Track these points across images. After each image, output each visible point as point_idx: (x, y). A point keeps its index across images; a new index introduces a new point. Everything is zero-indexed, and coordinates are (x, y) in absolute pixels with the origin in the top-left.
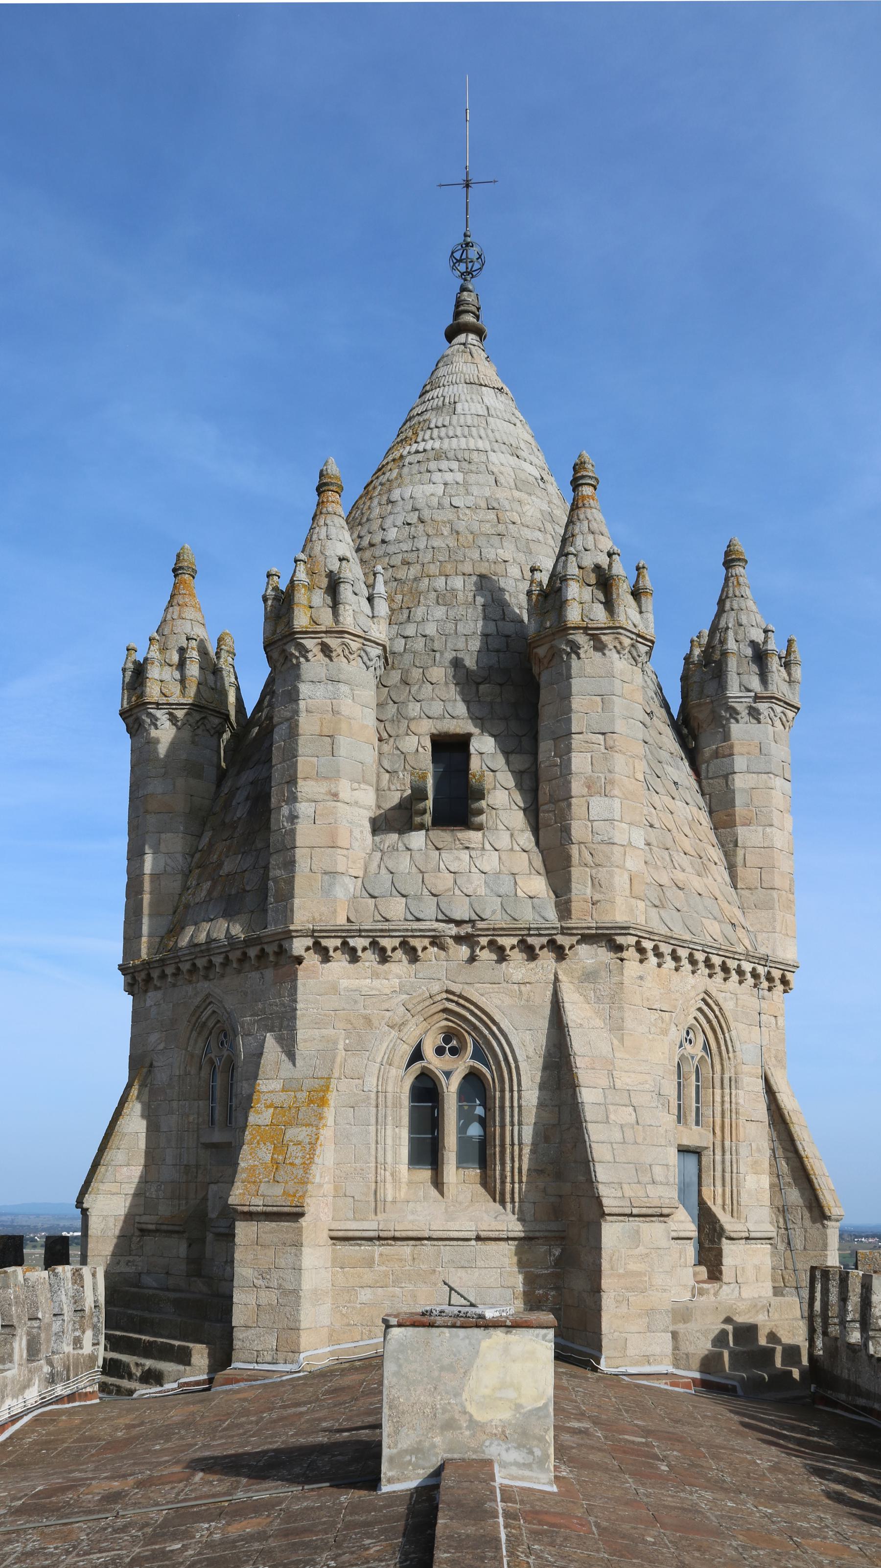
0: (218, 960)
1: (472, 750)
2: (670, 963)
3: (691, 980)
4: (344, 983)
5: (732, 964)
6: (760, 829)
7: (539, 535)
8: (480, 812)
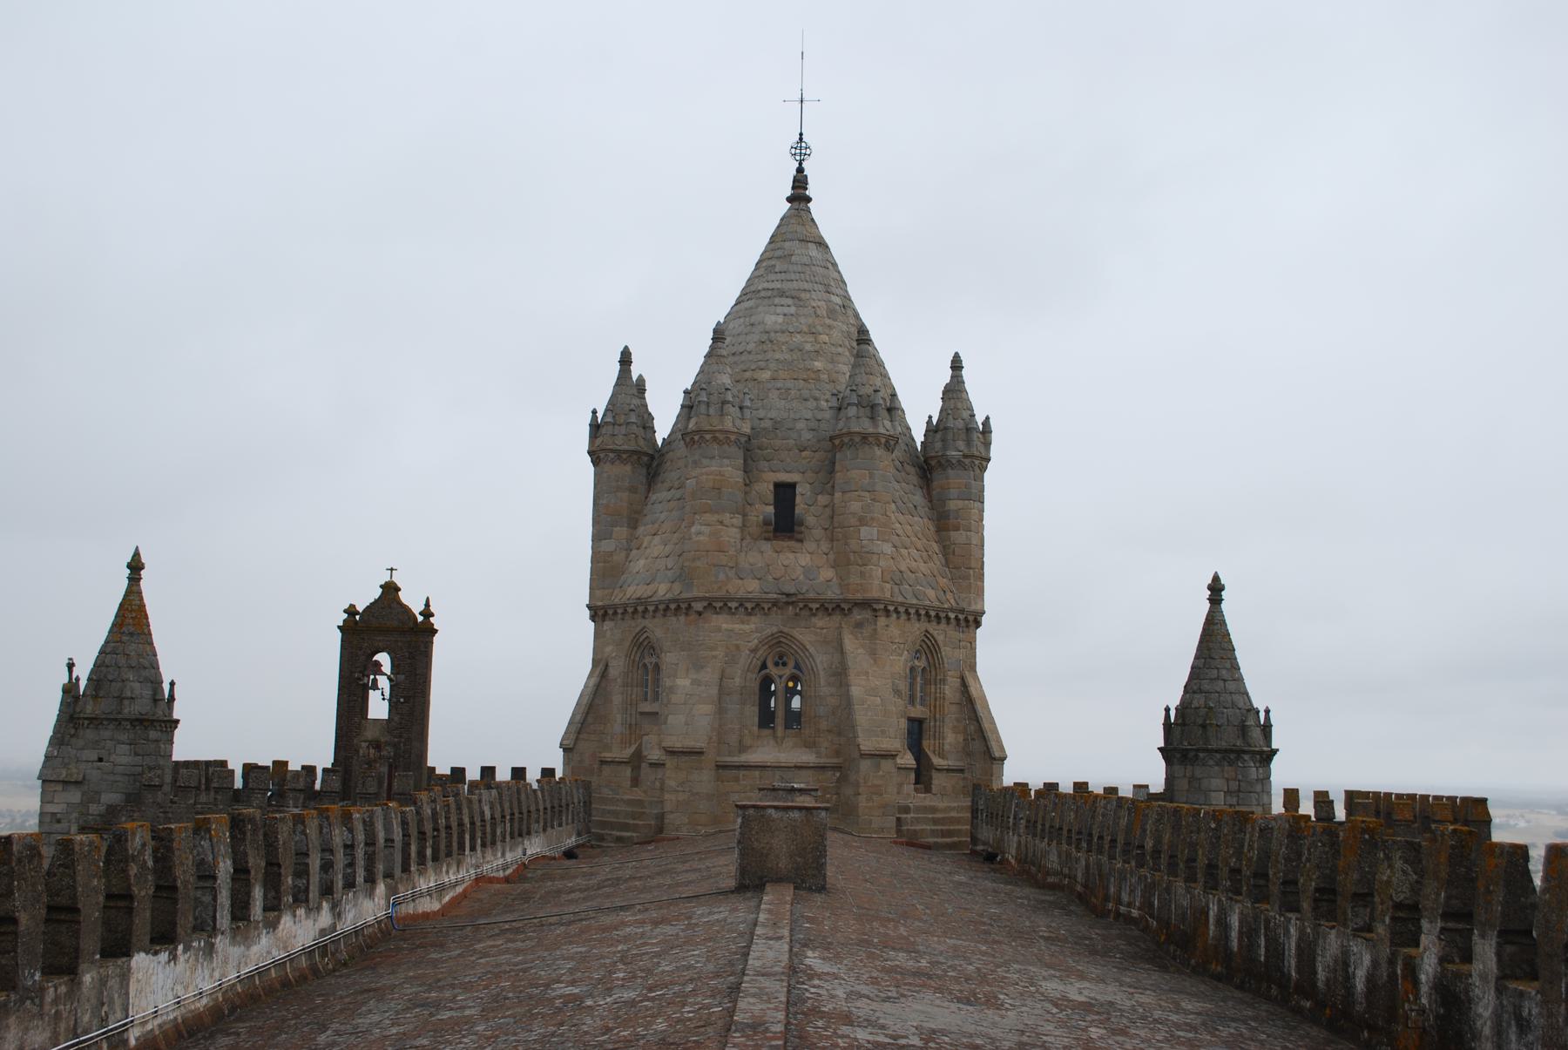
0: (651, 608)
1: (797, 492)
2: (904, 617)
3: (917, 625)
4: (724, 626)
5: (942, 615)
6: (964, 533)
7: (840, 350)
8: (801, 533)
